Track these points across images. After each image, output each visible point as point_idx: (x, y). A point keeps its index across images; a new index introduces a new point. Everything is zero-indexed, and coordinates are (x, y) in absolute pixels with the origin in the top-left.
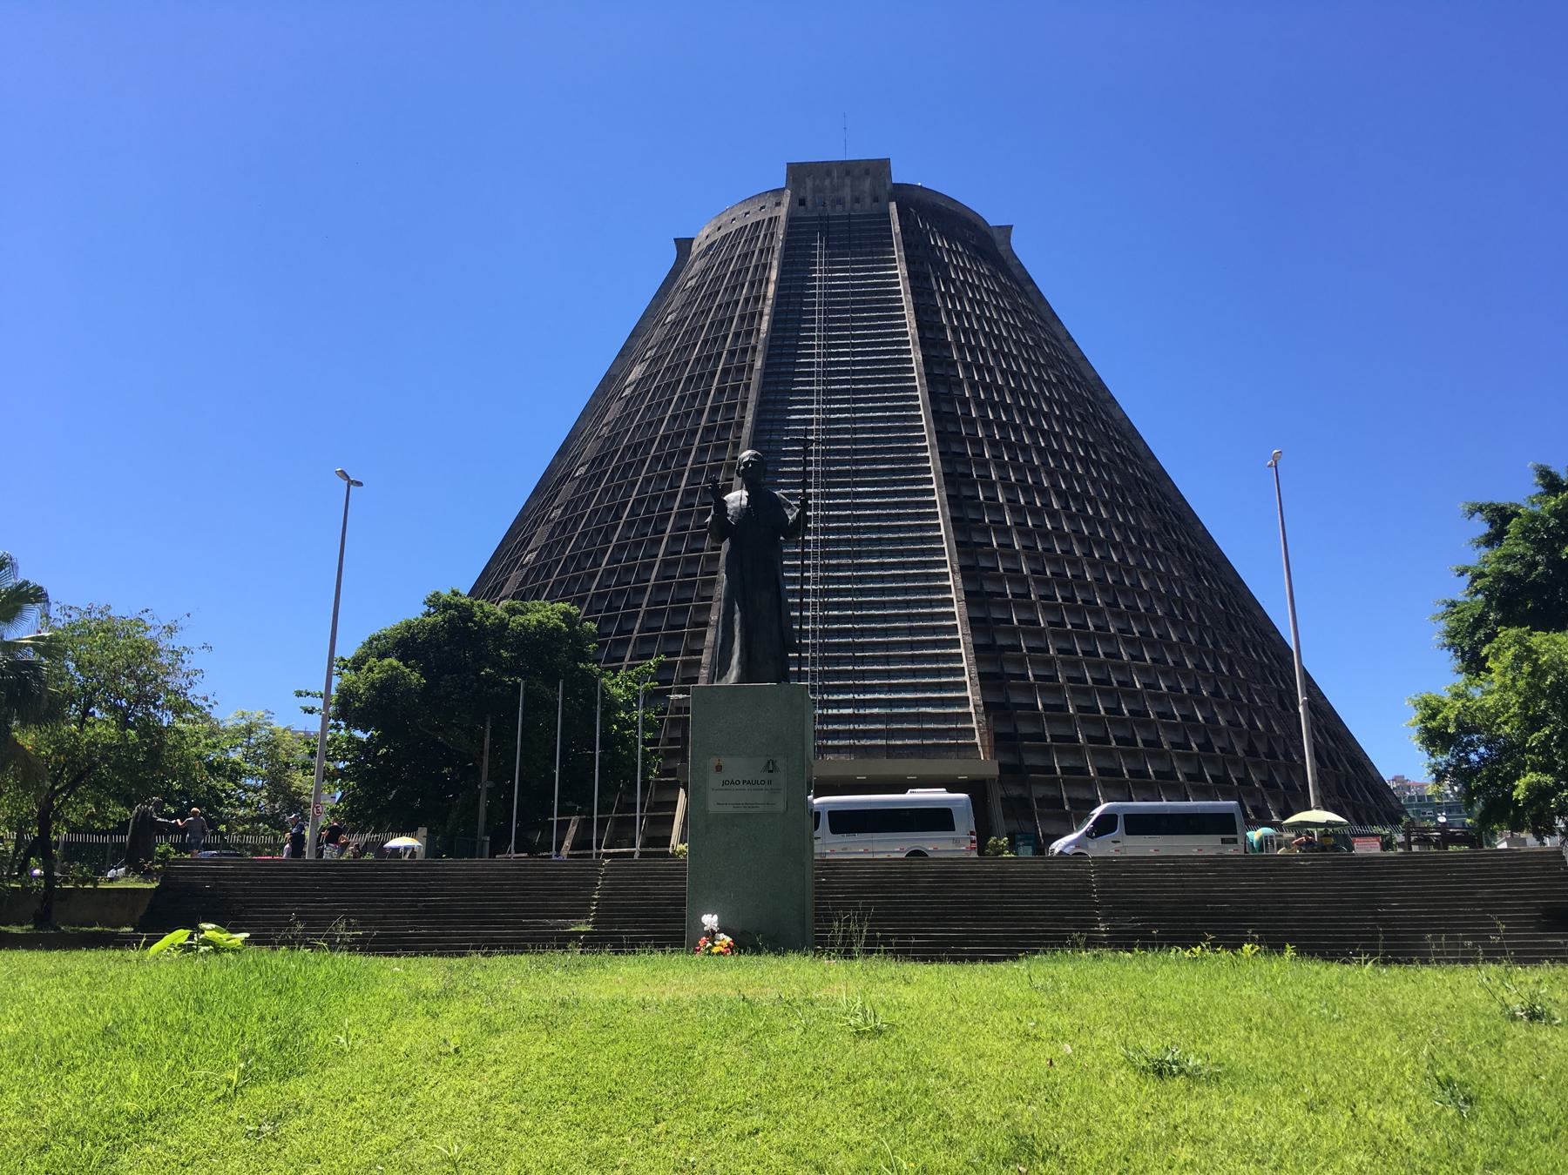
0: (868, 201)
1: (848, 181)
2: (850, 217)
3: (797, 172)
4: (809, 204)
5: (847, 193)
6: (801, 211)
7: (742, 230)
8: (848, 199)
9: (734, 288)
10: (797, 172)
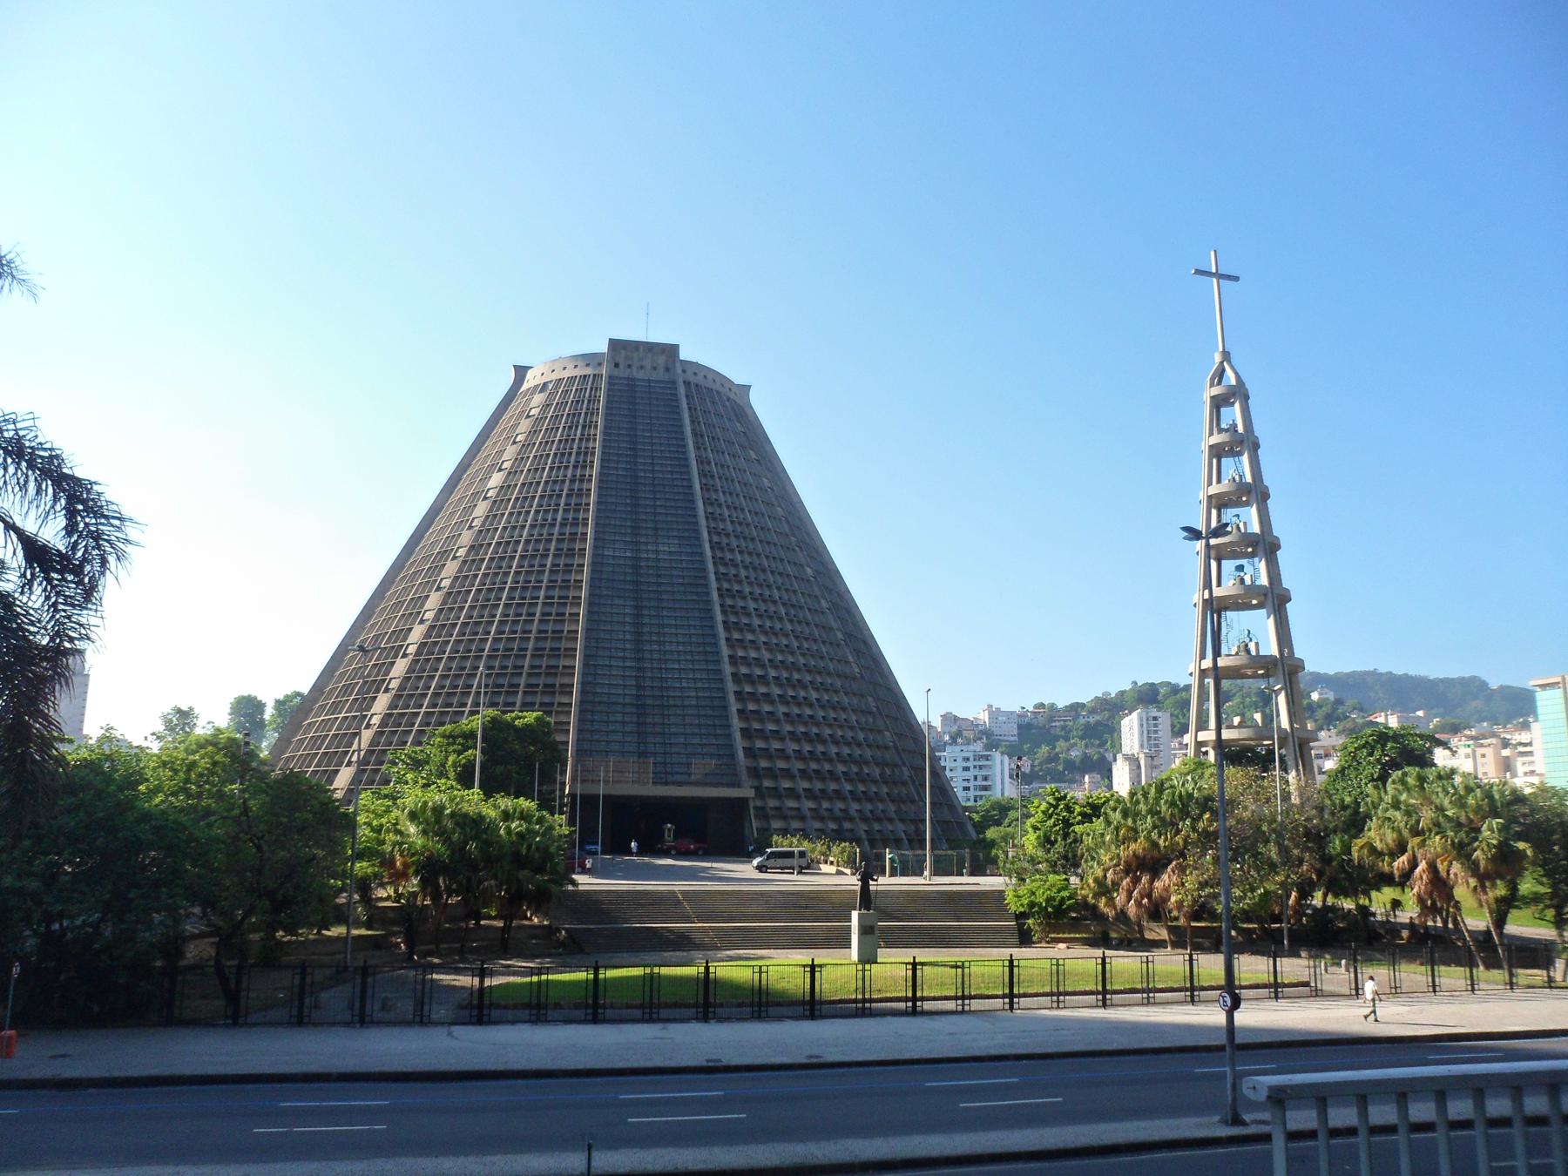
0: (662, 370)
1: (650, 355)
2: (649, 381)
3: (615, 344)
4: (621, 366)
5: (648, 364)
6: (616, 372)
7: (573, 379)
8: (649, 366)
9: (570, 428)
10: (615, 344)
